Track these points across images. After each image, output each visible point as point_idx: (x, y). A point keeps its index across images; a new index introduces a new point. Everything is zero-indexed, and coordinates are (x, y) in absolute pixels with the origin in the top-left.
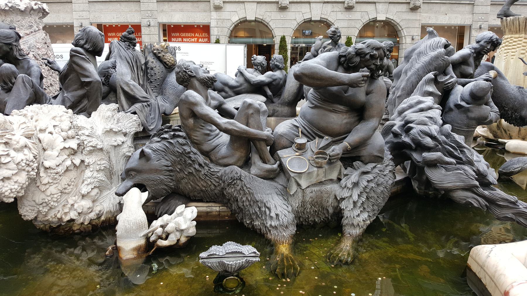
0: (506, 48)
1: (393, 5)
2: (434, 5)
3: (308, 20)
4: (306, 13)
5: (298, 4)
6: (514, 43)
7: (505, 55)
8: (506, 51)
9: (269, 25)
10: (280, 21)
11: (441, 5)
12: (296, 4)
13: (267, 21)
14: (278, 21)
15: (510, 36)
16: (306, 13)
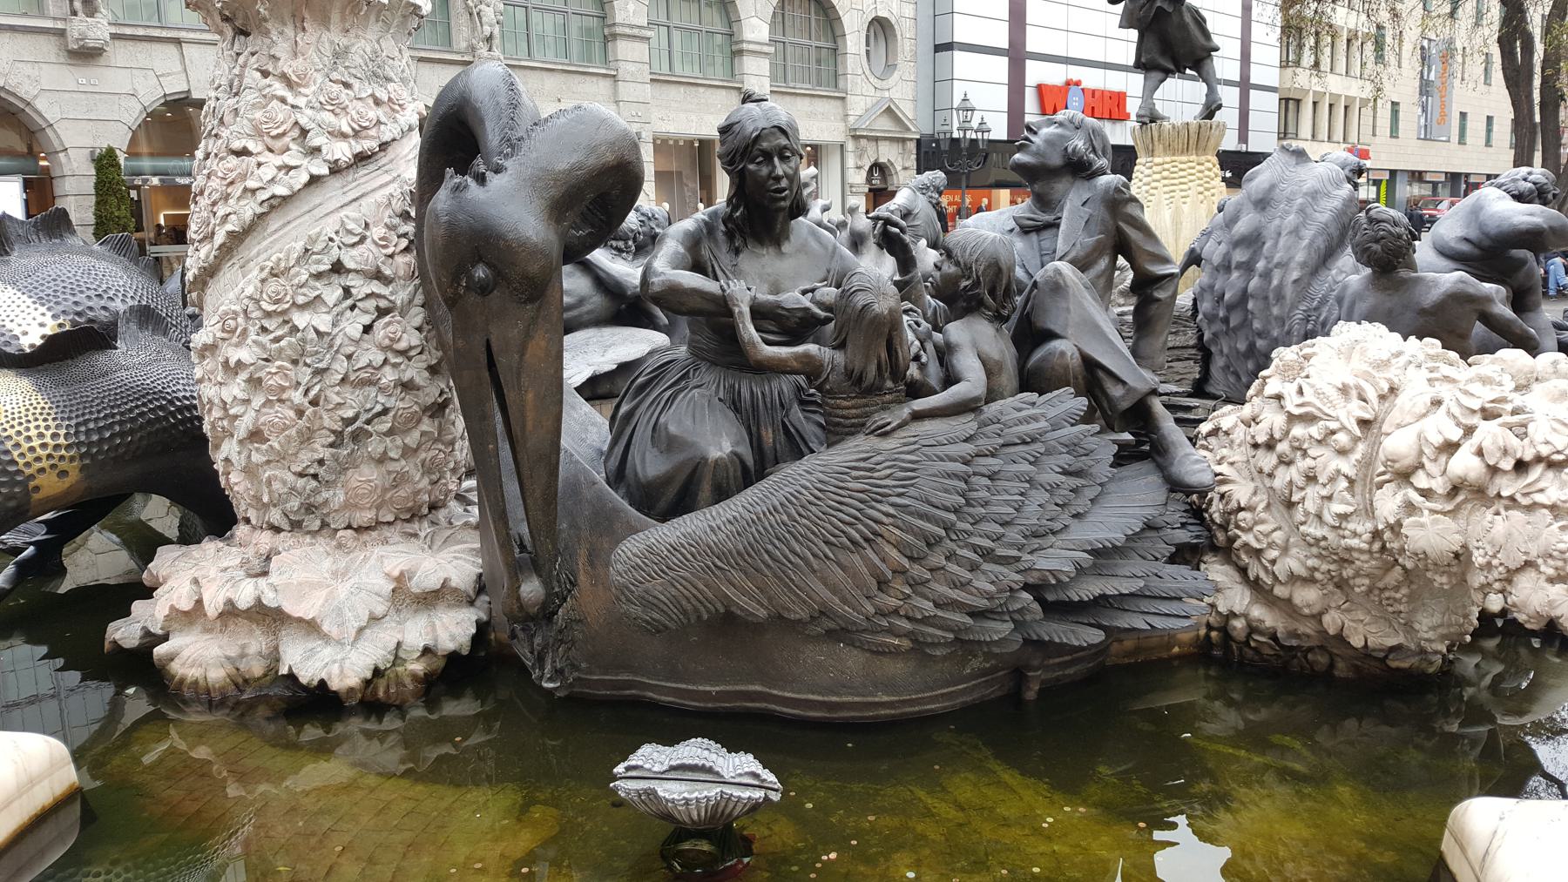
0: (1166, 182)
1: (428, 66)
2: (528, 72)
3: (176, 97)
4: (169, 74)
5: (138, 44)
6: (1182, 173)
7: (1167, 196)
8: (1166, 189)
9: (37, 111)
10: (74, 95)
11: (545, 74)
12: (131, 43)
13: (24, 96)
14: (67, 95)
15: (1168, 159)
16: (169, 74)
